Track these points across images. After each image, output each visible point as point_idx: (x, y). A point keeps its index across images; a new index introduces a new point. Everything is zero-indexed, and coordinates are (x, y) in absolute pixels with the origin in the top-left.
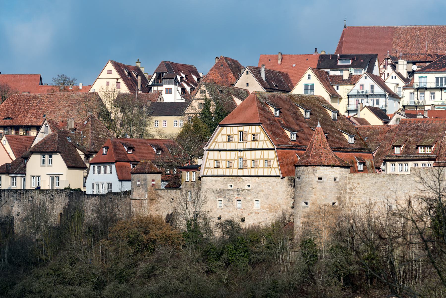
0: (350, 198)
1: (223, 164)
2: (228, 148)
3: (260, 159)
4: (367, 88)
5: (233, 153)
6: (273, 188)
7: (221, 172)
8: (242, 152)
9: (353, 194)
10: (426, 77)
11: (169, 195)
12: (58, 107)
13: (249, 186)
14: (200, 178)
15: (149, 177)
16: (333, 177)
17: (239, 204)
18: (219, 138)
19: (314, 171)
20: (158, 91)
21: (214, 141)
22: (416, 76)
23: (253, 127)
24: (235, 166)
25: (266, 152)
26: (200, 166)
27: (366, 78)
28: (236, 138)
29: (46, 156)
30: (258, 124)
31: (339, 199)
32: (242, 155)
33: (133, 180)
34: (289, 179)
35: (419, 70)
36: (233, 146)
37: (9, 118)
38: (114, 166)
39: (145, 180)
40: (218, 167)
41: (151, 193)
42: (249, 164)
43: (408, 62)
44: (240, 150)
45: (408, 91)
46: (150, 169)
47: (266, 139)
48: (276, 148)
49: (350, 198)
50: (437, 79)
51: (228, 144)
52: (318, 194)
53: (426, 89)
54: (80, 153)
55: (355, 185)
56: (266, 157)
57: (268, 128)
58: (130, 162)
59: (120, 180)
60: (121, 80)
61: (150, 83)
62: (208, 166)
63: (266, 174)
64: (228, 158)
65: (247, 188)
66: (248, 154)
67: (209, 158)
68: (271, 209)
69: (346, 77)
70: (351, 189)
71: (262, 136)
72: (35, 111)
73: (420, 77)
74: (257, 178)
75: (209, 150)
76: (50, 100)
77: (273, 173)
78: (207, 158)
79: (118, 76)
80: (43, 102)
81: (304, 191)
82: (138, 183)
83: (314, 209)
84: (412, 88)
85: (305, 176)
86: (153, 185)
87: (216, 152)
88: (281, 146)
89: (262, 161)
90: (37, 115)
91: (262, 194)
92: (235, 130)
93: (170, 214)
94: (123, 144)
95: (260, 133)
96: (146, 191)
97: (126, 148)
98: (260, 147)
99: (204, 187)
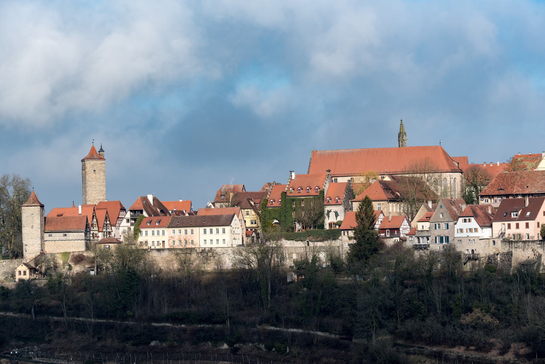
12: (536, 180)
37: (501, 189)
72: (519, 184)
80: (524, 177)
90: (521, 186)
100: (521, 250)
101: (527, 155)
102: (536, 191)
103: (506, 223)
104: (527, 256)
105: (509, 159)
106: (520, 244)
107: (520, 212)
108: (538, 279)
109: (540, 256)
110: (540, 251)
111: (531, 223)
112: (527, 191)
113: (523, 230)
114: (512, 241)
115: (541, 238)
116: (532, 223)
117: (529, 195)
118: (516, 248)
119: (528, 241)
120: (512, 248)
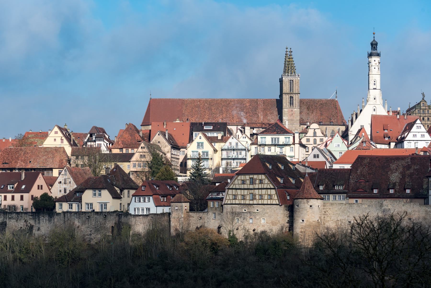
0: (324, 217)
1: (240, 197)
2: (242, 187)
3: (265, 194)
4: (234, 145)
5: (246, 192)
6: (274, 211)
7: (237, 202)
8: (252, 191)
9: (326, 215)
10: (265, 138)
11: (198, 215)
12: (38, 156)
13: (258, 210)
14: (222, 206)
15: (184, 204)
16: (317, 205)
17: (251, 221)
18: (236, 182)
19: (308, 202)
20: (91, 145)
21: (232, 184)
22: (259, 137)
23: (260, 176)
24: (248, 198)
25: (269, 190)
26: (223, 198)
27: (233, 138)
28: (248, 182)
29: (97, 191)
30: (264, 174)
31: (320, 217)
32: (252, 192)
33: (172, 206)
34: (285, 206)
35: (260, 133)
36: (246, 186)
37: (6, 163)
38: (151, 198)
39: (182, 206)
40: (235, 199)
41: (185, 214)
42: (257, 197)
43: (251, 128)
44: (251, 189)
45: (253, 147)
46: (184, 199)
47: (269, 183)
48: (276, 188)
49: (324, 217)
50: (272, 139)
51: (242, 185)
52: (310, 215)
53: (265, 145)
54: (117, 189)
55: (327, 210)
56: (269, 193)
57: (270, 176)
58: (159, 195)
59: (156, 206)
60: (63, 138)
61: (86, 140)
62: (228, 198)
63: (269, 203)
64: (242, 194)
65: (256, 211)
66: (257, 192)
67: (229, 193)
68: (273, 224)
69: (220, 138)
70: (325, 212)
71: (266, 181)
72: (23, 159)
73: (261, 138)
74: (263, 206)
75: (229, 189)
76: (32, 152)
77: (274, 202)
78: (227, 193)
79: (62, 135)
81: (302, 214)
82: (176, 208)
83: (308, 224)
84: (257, 144)
85: (302, 205)
86: (186, 209)
87: (234, 190)
88: (278, 186)
89: (266, 196)
90: (24, 161)
91: (267, 215)
92: (247, 177)
93: (199, 226)
94: (153, 184)
95: (265, 179)
96: (182, 213)
97: (155, 187)
98: (265, 187)
99: (225, 211)
100: (15, 220)
101: (37, 133)
102: (38, 167)
103: (3, 195)
104: (20, 226)
105: (17, 135)
106: (14, 215)
107: (16, 185)
108: (25, 249)
109: (31, 227)
110: (32, 222)
111: (26, 195)
112: (29, 166)
113: (17, 202)
114: (7, 212)
115: (34, 210)
116: (26, 196)
117: (26, 169)
118: (10, 218)
119: (21, 213)
120: (6, 218)
